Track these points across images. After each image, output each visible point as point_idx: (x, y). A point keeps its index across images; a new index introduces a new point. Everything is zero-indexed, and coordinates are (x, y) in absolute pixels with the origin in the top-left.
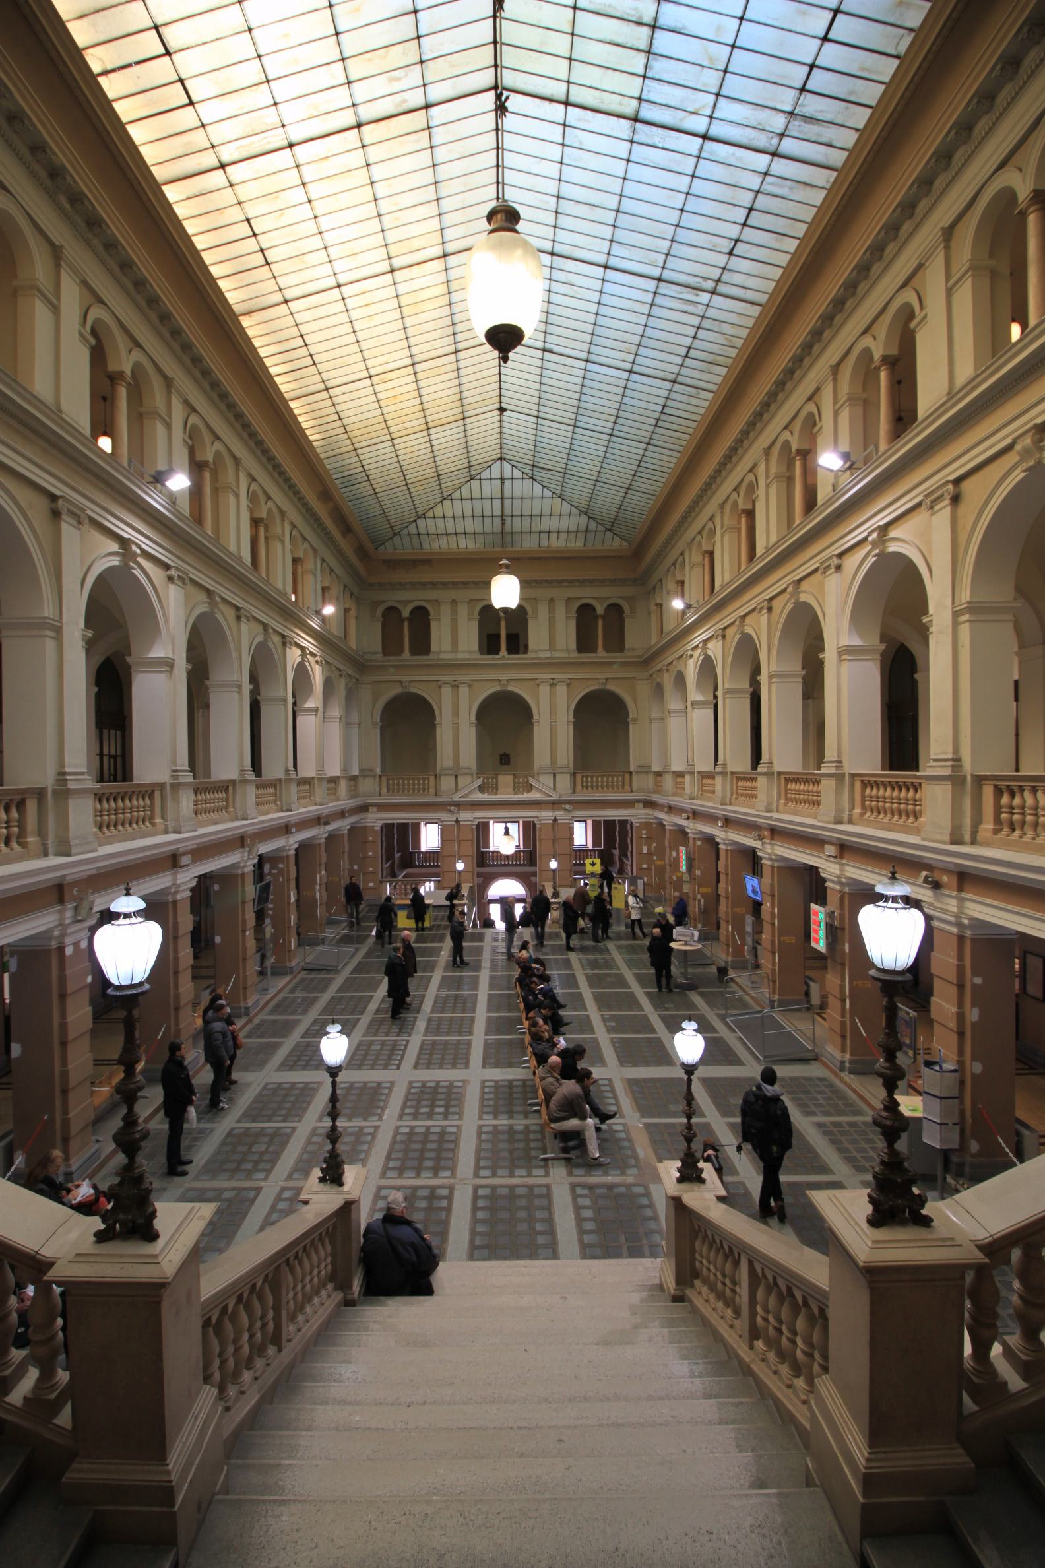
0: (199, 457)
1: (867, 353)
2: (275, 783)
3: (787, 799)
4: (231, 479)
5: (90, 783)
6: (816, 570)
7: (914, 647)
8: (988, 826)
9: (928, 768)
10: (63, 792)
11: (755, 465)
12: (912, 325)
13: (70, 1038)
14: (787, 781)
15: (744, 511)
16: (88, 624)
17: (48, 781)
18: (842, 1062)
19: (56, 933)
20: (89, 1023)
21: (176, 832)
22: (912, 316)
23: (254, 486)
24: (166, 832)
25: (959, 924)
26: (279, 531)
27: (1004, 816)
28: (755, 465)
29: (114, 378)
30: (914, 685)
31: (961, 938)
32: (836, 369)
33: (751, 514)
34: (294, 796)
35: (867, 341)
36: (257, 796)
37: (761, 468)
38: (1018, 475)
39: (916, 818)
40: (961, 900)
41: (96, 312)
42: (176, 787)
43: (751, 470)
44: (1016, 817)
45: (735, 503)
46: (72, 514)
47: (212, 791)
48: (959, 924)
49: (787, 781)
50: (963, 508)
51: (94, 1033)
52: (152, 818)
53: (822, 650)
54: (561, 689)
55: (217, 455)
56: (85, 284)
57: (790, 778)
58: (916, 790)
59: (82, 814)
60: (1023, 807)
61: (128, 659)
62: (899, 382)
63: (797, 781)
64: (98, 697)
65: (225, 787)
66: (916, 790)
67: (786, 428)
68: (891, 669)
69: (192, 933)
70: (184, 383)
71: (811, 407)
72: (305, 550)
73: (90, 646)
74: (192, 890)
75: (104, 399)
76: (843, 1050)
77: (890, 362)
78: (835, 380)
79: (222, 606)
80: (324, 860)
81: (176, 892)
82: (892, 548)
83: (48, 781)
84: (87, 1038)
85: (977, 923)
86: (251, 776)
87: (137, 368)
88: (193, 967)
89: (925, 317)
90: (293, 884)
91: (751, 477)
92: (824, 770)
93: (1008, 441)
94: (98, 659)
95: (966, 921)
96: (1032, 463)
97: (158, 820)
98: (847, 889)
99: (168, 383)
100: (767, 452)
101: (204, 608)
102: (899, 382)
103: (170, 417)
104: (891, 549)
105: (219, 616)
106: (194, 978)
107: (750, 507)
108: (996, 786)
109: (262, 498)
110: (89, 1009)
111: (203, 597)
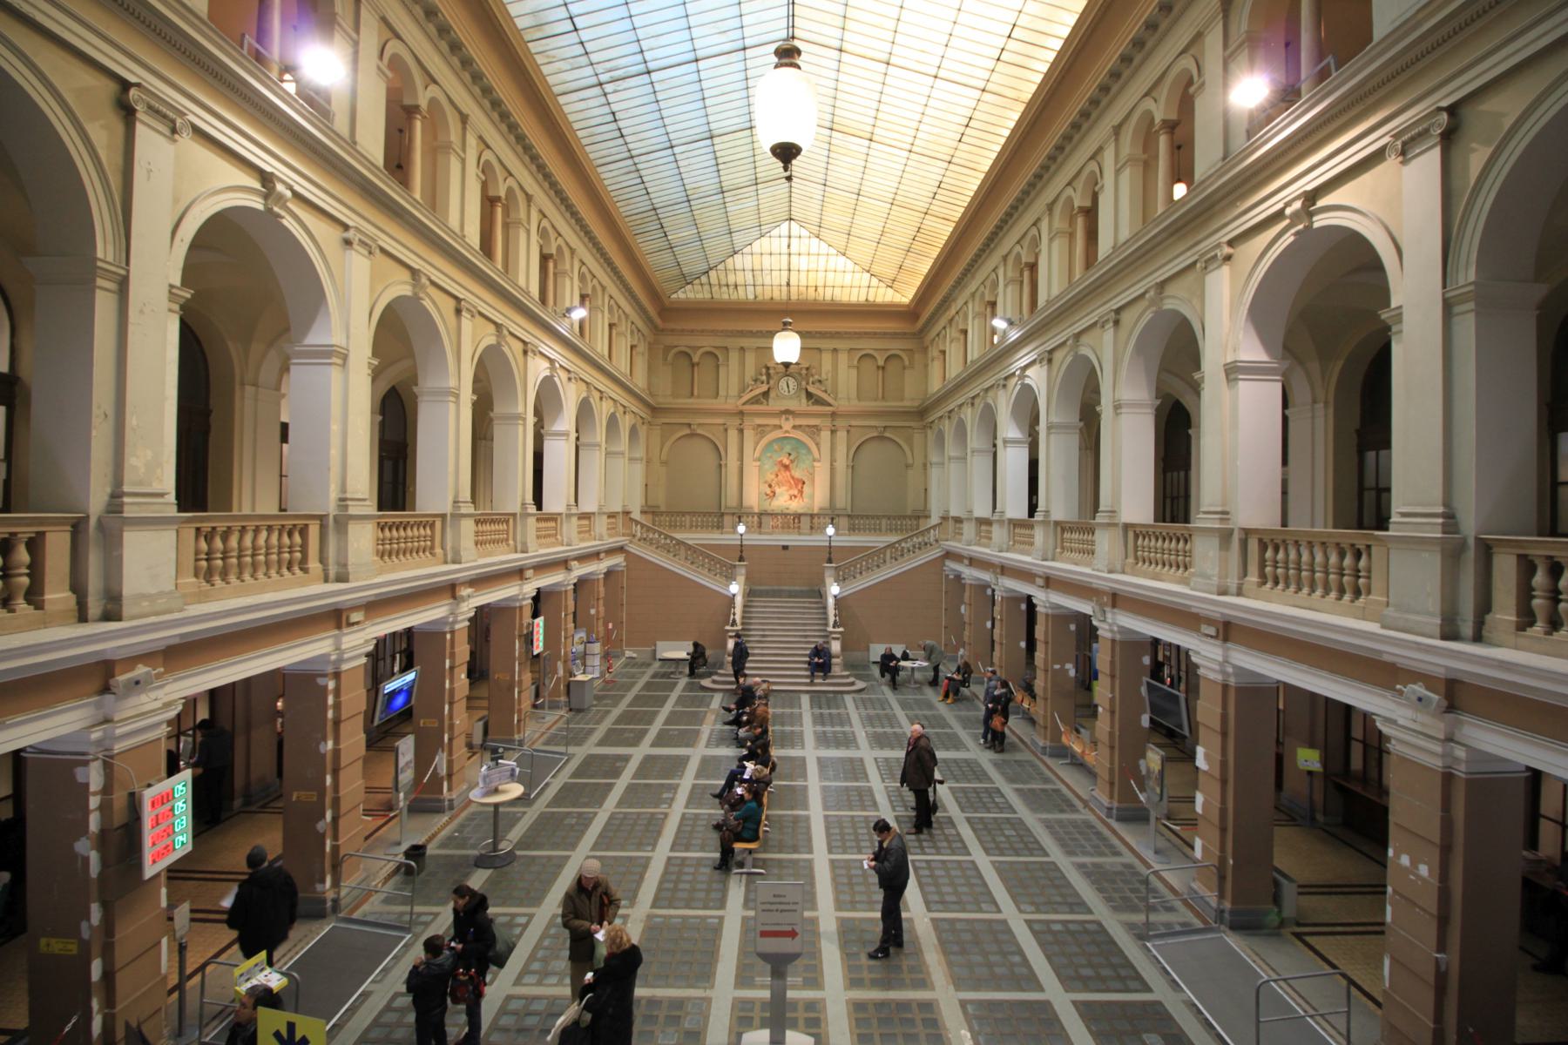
0: (491, 193)
1: (1149, 117)
2: (553, 518)
3: (1063, 548)
4: (523, 215)
5: (371, 508)
6: (1095, 324)
7: (1187, 401)
8: (1253, 578)
9: (1199, 521)
10: (342, 522)
11: (1039, 219)
12: (1192, 90)
13: (343, 764)
14: (1063, 530)
15: (1027, 264)
16: (375, 354)
17: (332, 509)
18: (1110, 809)
19: (333, 657)
20: (362, 750)
21: (454, 562)
22: (1190, 82)
23: (545, 223)
24: (446, 562)
25: (1224, 672)
26: (568, 267)
27: (1268, 569)
28: (1039, 219)
29: (411, 111)
30: (1189, 437)
31: (1225, 687)
32: (1117, 130)
33: (1033, 267)
34: (574, 530)
35: (1149, 104)
36: (538, 529)
37: (1044, 225)
38: (1288, 239)
39: (1186, 568)
40: (1226, 650)
41: (394, 47)
42: (458, 517)
43: (1034, 224)
44: (1280, 571)
45: (1018, 256)
46: (362, 242)
47: (494, 524)
48: (1224, 672)
49: (1063, 530)
50: (1123, 332)
51: (366, 760)
52: (432, 547)
53: (1099, 403)
54: (842, 435)
55: (510, 191)
56: (384, 20)
57: (1062, 527)
58: (1186, 541)
59: (362, 540)
60: (1286, 562)
61: (415, 389)
62: (1179, 147)
63: (1071, 530)
64: (382, 425)
65: (506, 518)
66: (1186, 541)
67: (1069, 184)
68: (1167, 423)
69: (469, 663)
70: (481, 121)
71: (1093, 166)
72: (594, 288)
73: (376, 375)
74: (470, 620)
75: (401, 131)
76: (1111, 797)
77: (1170, 127)
78: (1117, 140)
79: (510, 339)
80: (602, 595)
81: (455, 622)
82: (1169, 305)
83: (332, 509)
84: (360, 762)
85: (1240, 671)
86: (532, 509)
87: (433, 102)
88: (469, 698)
89: (1203, 84)
90: (571, 617)
91: (1034, 231)
92: (1098, 520)
93: (1281, 205)
94: (384, 387)
95: (1230, 670)
96: (1301, 227)
97: (438, 550)
98: (1118, 637)
99: (464, 119)
100: (1050, 207)
101: (491, 340)
102: (1179, 147)
103: (464, 151)
104: (1166, 307)
105: (506, 349)
106: (468, 708)
107: (1032, 260)
108: (1260, 540)
109: (553, 235)
110: (363, 736)
111: (491, 329)
